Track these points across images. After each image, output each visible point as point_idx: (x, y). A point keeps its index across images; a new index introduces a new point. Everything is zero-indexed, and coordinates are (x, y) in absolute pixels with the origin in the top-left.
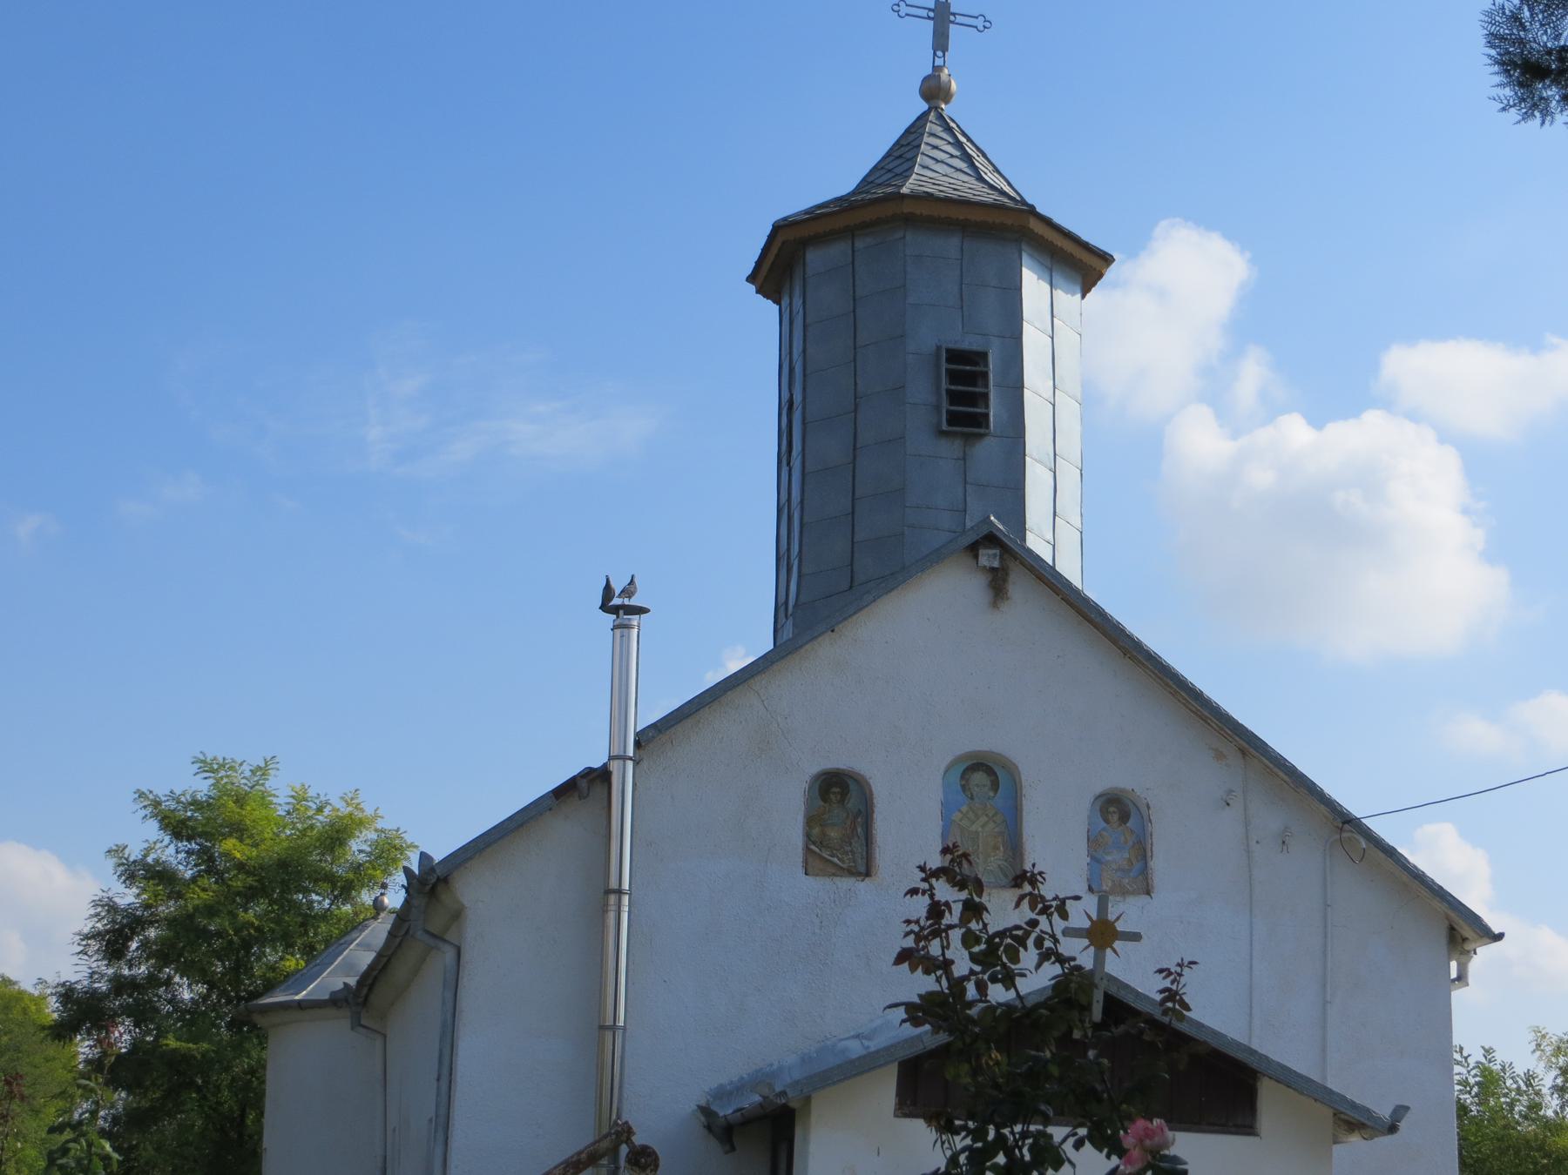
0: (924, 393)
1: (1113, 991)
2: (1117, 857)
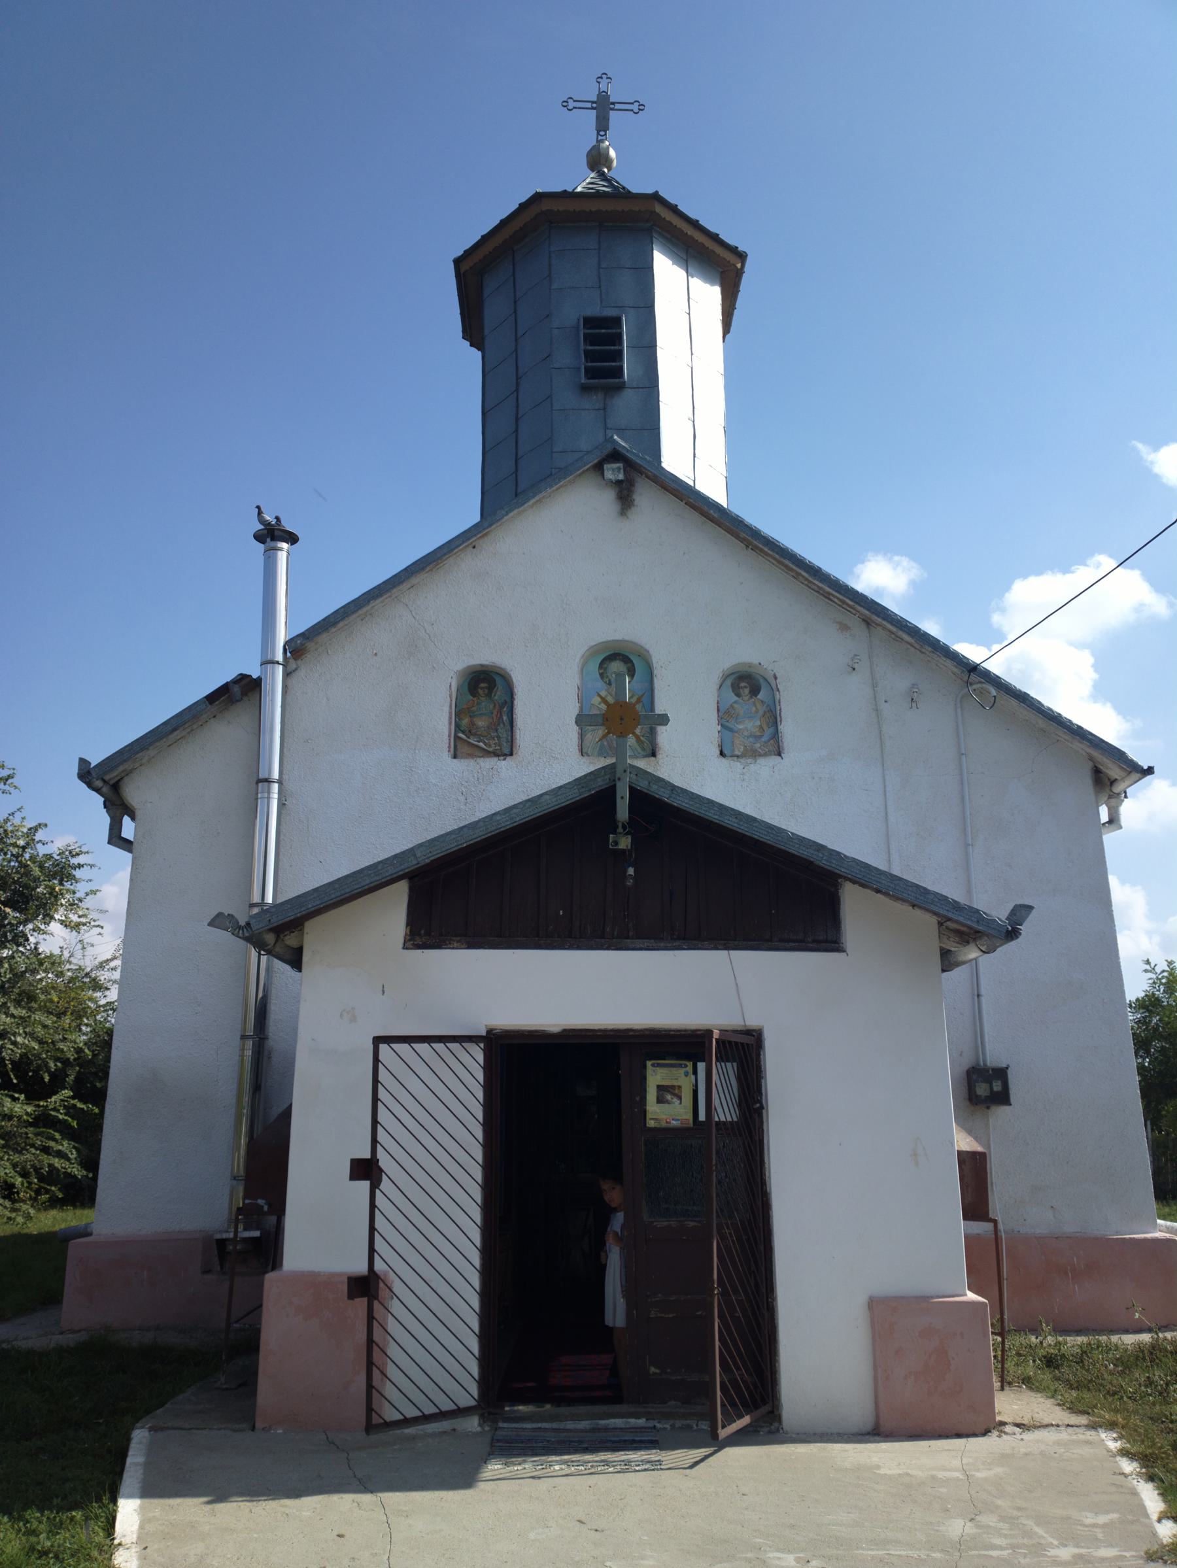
0: (568, 357)
1: (642, 785)
2: (749, 726)
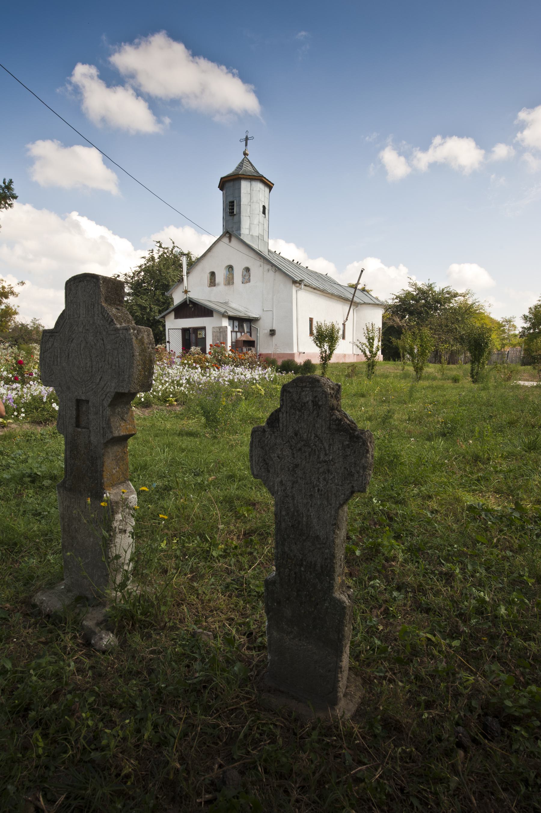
2: (247, 277)
